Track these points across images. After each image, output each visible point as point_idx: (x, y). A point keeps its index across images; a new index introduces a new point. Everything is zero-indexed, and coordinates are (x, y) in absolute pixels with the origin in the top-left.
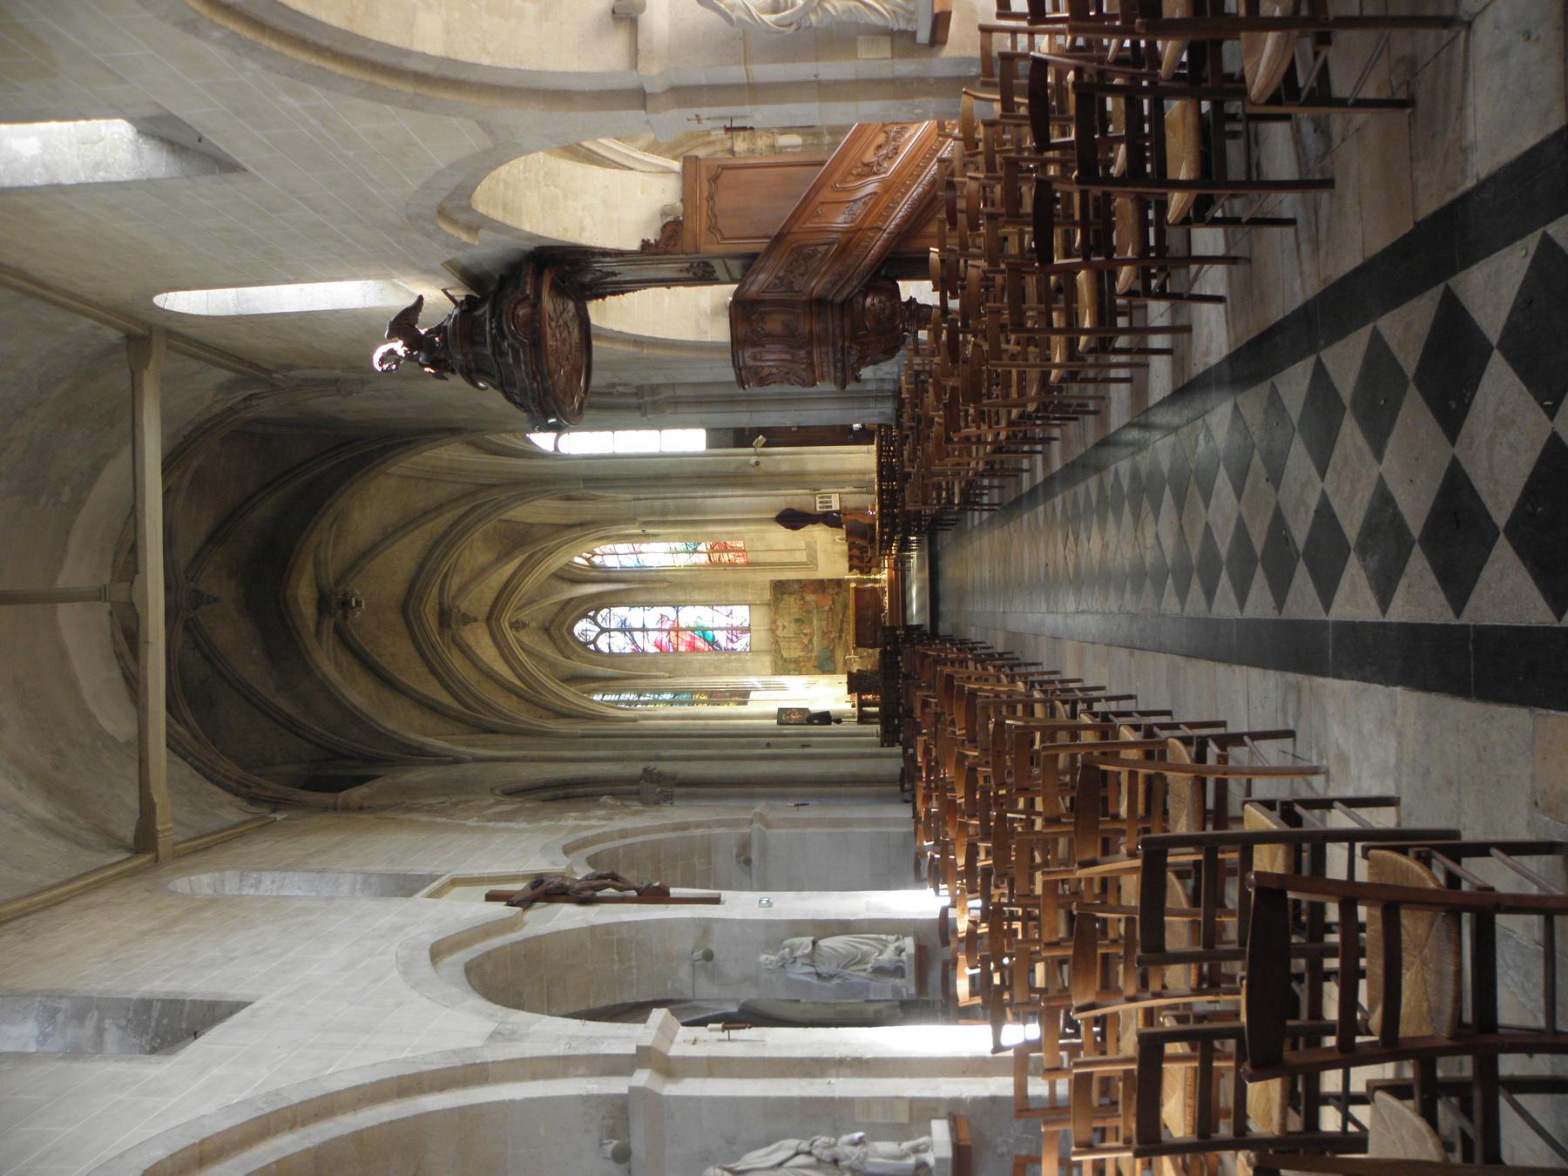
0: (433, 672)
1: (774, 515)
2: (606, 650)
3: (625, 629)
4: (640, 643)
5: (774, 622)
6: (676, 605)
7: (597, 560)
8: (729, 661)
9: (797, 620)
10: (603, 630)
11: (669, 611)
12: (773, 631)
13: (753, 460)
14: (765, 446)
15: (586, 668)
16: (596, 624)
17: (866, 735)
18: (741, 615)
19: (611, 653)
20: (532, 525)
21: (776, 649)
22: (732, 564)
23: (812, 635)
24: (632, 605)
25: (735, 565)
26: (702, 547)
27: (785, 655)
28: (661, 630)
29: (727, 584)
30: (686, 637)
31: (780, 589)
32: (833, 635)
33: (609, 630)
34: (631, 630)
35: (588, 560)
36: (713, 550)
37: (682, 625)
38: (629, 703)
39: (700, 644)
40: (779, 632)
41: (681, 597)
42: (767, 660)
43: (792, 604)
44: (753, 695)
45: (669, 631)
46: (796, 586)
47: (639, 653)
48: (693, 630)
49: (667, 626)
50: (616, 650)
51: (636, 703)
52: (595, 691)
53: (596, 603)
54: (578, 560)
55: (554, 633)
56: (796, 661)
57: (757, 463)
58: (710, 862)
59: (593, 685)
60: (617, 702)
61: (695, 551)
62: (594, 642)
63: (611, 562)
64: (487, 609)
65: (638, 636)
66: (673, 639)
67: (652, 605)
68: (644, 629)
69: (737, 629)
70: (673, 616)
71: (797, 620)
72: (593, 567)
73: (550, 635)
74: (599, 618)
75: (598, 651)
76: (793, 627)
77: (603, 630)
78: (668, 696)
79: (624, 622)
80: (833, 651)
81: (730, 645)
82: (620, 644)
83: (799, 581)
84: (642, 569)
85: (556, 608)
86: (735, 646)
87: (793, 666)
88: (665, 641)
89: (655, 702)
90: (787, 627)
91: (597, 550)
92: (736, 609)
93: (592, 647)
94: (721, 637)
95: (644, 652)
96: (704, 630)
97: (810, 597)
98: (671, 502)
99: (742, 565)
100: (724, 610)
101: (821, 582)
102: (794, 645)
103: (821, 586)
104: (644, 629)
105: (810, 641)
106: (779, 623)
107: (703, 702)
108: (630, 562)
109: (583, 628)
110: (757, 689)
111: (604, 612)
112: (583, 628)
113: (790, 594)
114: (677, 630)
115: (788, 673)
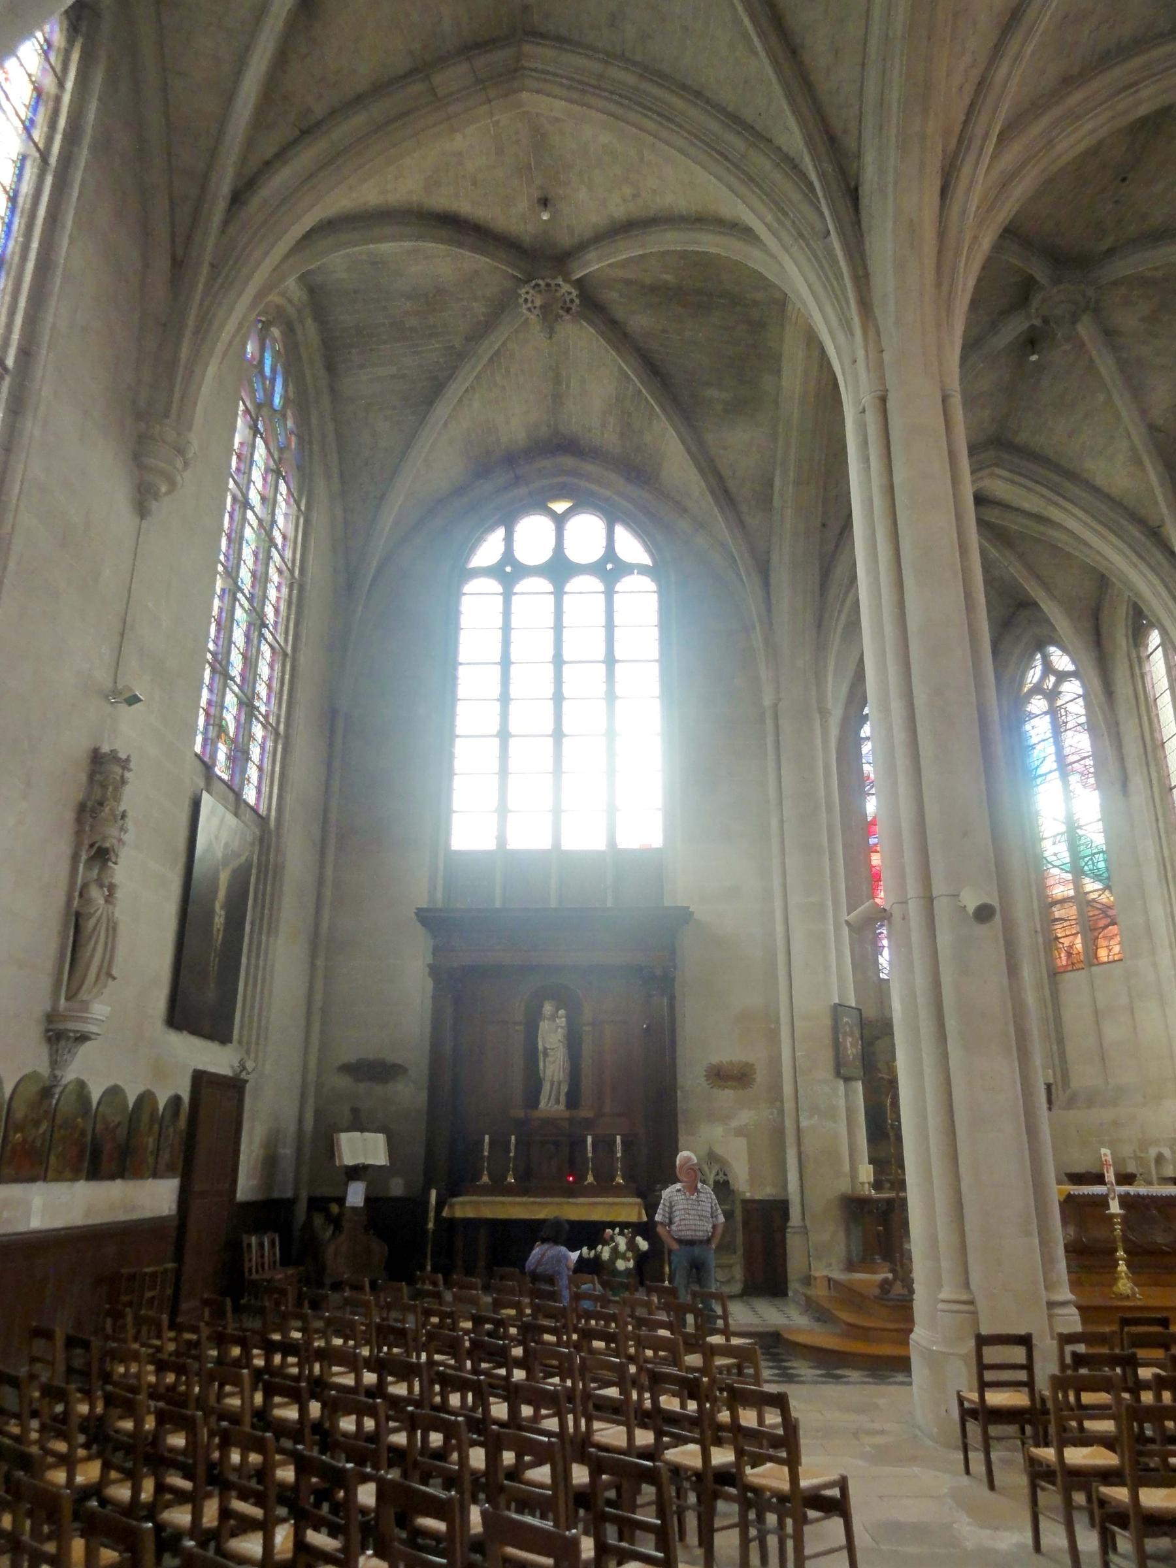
7: (1038, 704)
35: (1037, 689)
36: (1081, 899)
61: (1078, 872)
63: (1038, 729)
64: (1022, 438)
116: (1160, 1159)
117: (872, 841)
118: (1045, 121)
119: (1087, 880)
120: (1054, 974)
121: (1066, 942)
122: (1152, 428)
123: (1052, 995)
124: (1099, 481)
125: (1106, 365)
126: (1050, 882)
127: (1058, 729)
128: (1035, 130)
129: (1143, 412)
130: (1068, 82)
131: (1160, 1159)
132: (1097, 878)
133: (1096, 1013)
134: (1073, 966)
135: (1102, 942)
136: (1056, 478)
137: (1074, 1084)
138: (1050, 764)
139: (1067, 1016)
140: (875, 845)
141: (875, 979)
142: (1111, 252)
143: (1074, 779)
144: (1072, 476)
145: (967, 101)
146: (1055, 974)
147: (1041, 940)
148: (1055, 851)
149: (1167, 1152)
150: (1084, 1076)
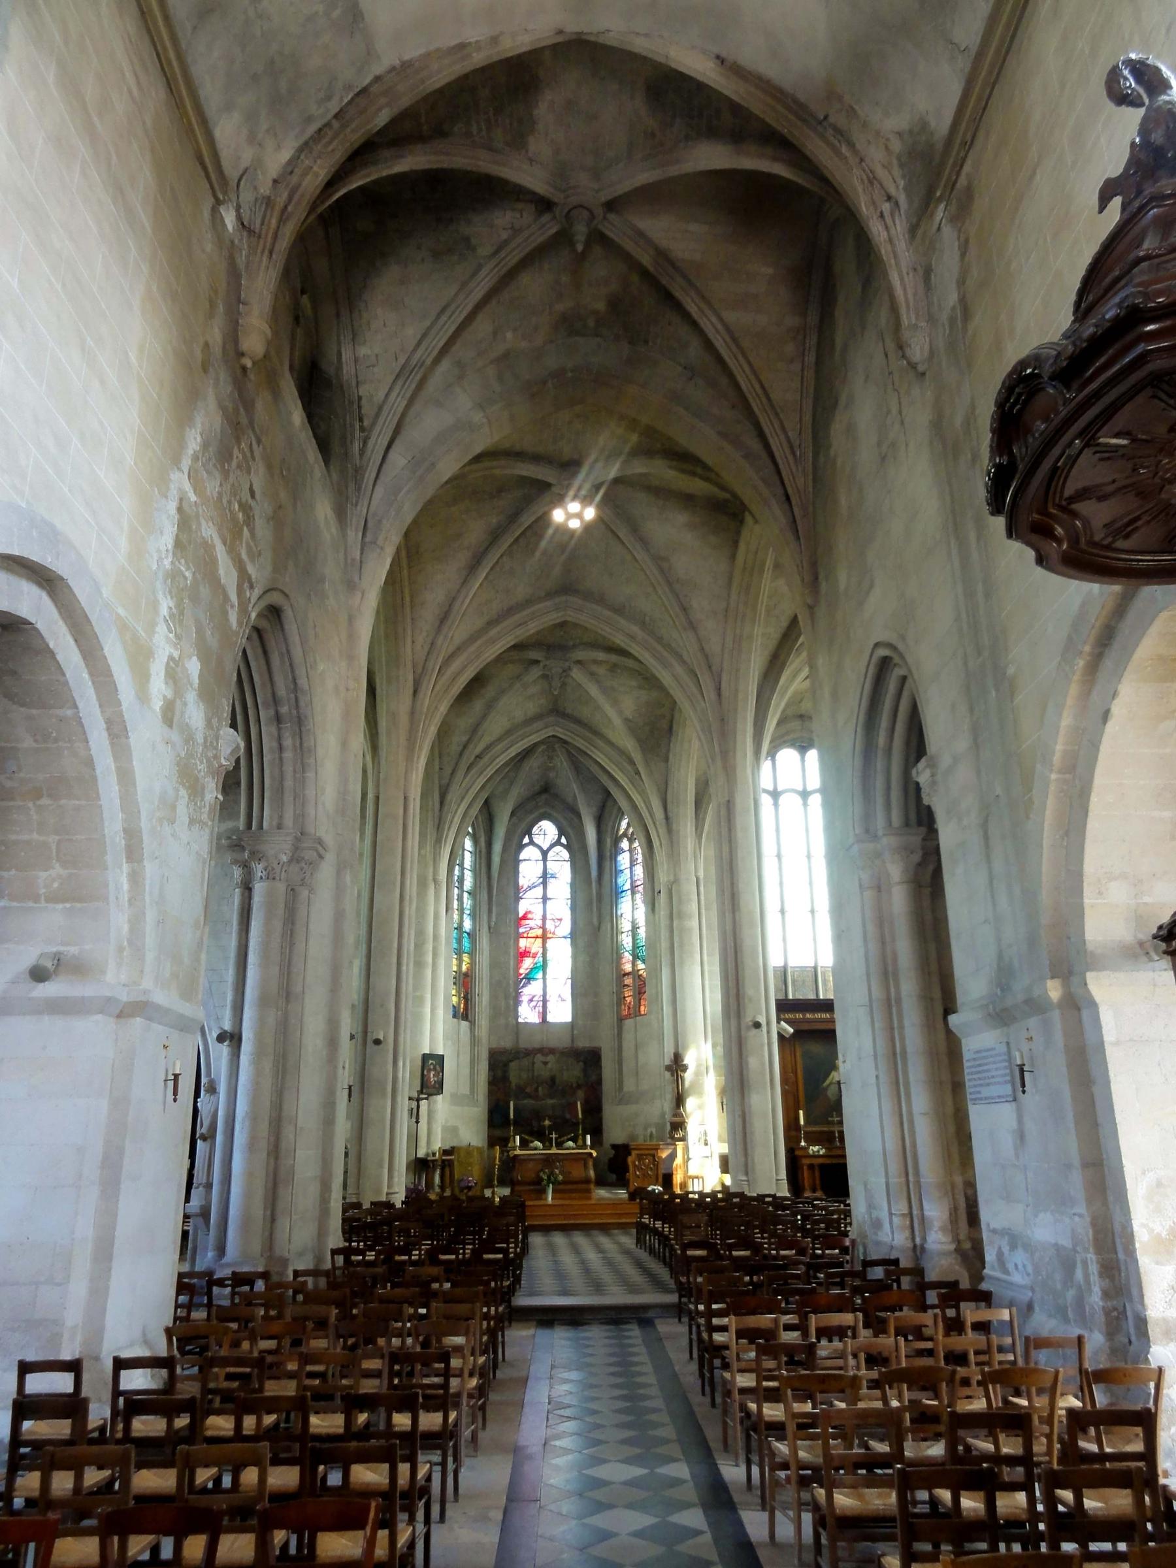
0: (491, 624)
2: (523, 855)
3: (545, 877)
4: (529, 894)
5: (552, 1051)
6: (573, 936)
7: (625, 844)
8: (507, 997)
9: (553, 1079)
10: (545, 854)
11: (566, 928)
12: (541, 1051)
13: (762, 1020)
14: (781, 1037)
15: (500, 831)
16: (552, 846)
17: (390, 1177)
18: (561, 1012)
19: (517, 862)
20: (667, 760)
21: (518, 1054)
22: (621, 999)
24: (573, 885)
25: (619, 1004)
26: (641, 965)
27: (513, 1065)
28: (544, 918)
29: (596, 995)
30: (536, 946)
31: (591, 1059)
33: (545, 859)
34: (544, 884)
35: (625, 835)
36: (634, 973)
37: (549, 943)
38: (461, 880)
39: (527, 963)
40: (539, 1058)
42: (507, 1043)
43: (574, 1073)
44: (465, 1024)
45: (543, 928)
46: (594, 1078)
47: (517, 894)
49: (550, 926)
50: (523, 867)
51: (461, 887)
52: (475, 841)
53: (576, 846)
54: (624, 824)
55: (544, 796)
56: (505, 1079)
57: (757, 1025)
58: (53, 898)
59: (482, 840)
60: (461, 866)
61: (635, 957)
62: (532, 843)
63: (624, 860)
64: (569, 711)
65: (539, 891)
66: (532, 933)
67: (573, 909)
68: (545, 899)
72: (617, 840)
73: (540, 793)
74: (558, 848)
75: (521, 847)
76: (545, 1073)
77: (545, 854)
78: (467, 925)
79: (553, 877)
81: (525, 999)
82: (529, 869)
84: (617, 893)
85: (570, 800)
87: (499, 1073)
88: (531, 923)
89: (461, 911)
90: (545, 1067)
91: (636, 844)
93: (526, 840)
94: (532, 990)
95: (518, 899)
96: (544, 967)
98: (695, 923)
99: (619, 1012)
102: (524, 1075)
103: (594, 1109)
104: (545, 899)
105: (529, 1096)
106: (551, 1058)
107: (460, 966)
108: (624, 881)
109: (546, 831)
110: (472, 1030)
111: (566, 854)
112: (546, 831)
113: (585, 1071)
114: (544, 938)
115: (492, 1067)
116: (651, 1135)
117: (521, 930)
118: (479, 642)
119: (639, 962)
120: (621, 1020)
121: (628, 999)
122: (627, 720)
124: (614, 740)
125: (593, 690)
126: (624, 961)
127: (632, 865)
128: (472, 649)
129: (620, 712)
130: (491, 624)
131: (651, 1135)
132: (644, 961)
133: (636, 1046)
134: (629, 1016)
135: (643, 1002)
136: (590, 735)
137: (625, 1089)
138: (627, 886)
139: (625, 1044)
142: (574, 646)
143: (638, 896)
144: (596, 733)
145: (426, 650)
148: (626, 941)
149: (654, 1131)
150: (629, 1085)
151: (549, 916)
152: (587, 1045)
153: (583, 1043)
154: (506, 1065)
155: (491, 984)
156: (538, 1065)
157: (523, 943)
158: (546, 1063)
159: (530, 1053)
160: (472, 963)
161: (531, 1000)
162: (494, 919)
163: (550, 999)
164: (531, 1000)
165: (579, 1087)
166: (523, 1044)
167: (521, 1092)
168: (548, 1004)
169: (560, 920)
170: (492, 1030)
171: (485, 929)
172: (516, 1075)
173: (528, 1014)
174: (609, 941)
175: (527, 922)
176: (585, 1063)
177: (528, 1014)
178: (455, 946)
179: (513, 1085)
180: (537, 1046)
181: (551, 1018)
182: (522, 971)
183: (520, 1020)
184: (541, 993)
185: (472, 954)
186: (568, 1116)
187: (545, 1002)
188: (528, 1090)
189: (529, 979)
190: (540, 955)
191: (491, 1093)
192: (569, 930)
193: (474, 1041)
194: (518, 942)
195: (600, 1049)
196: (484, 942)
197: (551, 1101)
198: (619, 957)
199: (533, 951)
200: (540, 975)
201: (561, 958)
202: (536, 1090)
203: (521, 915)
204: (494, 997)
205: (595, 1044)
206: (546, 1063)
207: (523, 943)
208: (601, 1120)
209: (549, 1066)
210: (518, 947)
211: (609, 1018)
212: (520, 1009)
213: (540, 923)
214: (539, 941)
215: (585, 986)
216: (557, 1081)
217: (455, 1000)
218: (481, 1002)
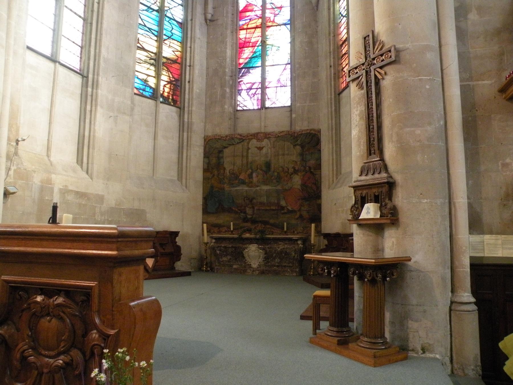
1: (380, 27)
5: (267, 136)
9: (268, 165)
11: (285, 15)
12: (255, 136)
18: (280, 97)
23: (250, 184)
27: (227, 152)
28: (264, 8)
29: (315, 74)
30: (256, 36)
32: (249, 211)
37: (269, 32)
39: (247, 53)
41: (298, 24)
43: (291, 156)
45: (263, 17)
46: (312, 162)
48: (264, 43)
49: (268, 14)
56: (219, 165)
69: (263, 94)
70: (279, 20)
71: (268, 165)
76: (259, 159)
80: (230, 210)
81: (244, 87)
83: (319, 166)
86: (244, 93)
87: (214, 161)
90: (260, 153)
92: (288, 89)
94: (253, 77)
96: (263, 56)
97: (297, 180)
100: (286, 76)
101: (318, 196)
102: (239, 162)
105: (243, 183)
106: (265, 142)
107: (160, 48)
110: (181, 116)
113: (302, 155)
114: (264, 27)
115: (207, 155)
117: (241, 23)
123: (335, 110)
137: (343, 171)
140: (243, 25)
141: (231, 110)
146: (339, 94)
147: (333, 71)
151: (269, 6)
152: (303, 128)
153: (301, 126)
154: (221, 152)
155: (207, 74)
156: (253, 150)
157: (243, 34)
158: (260, 149)
159: (244, 139)
160: (184, 51)
161: (250, 89)
162: (210, 10)
163: (271, 83)
164: (250, 89)
165: (296, 172)
166: (240, 131)
167: (235, 178)
168: (268, 91)
169: (281, 8)
170: (207, 118)
171: (199, 19)
172: (230, 161)
173: (247, 102)
174: (325, 13)
175: (248, 14)
176: (303, 147)
177: (247, 102)
178: (156, 28)
179: (227, 171)
180: (253, 131)
181: (268, 104)
182: (241, 61)
183: (239, 108)
184: (259, 80)
185: (183, 43)
186: (283, 203)
187: (263, 88)
188: (242, 177)
189: (248, 68)
190: (259, 43)
191: (205, 179)
192: (289, 18)
193: (184, 127)
194: (237, 34)
195: (319, 131)
196: (199, 33)
197: (265, 188)
198: (337, 26)
199: (253, 40)
200: (259, 63)
201: (280, 42)
202: (250, 176)
203: (241, 8)
204: (210, 86)
205: (315, 127)
206: (260, 149)
207: (243, 34)
208: (319, 207)
209: (264, 151)
210: (238, 38)
211: (326, 95)
212: (239, 98)
213: (259, 13)
214: (258, 31)
215: (302, 67)
216: (272, 165)
217: (152, 82)
218: (191, 89)
